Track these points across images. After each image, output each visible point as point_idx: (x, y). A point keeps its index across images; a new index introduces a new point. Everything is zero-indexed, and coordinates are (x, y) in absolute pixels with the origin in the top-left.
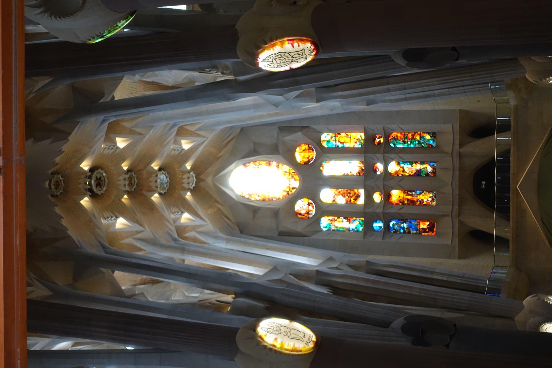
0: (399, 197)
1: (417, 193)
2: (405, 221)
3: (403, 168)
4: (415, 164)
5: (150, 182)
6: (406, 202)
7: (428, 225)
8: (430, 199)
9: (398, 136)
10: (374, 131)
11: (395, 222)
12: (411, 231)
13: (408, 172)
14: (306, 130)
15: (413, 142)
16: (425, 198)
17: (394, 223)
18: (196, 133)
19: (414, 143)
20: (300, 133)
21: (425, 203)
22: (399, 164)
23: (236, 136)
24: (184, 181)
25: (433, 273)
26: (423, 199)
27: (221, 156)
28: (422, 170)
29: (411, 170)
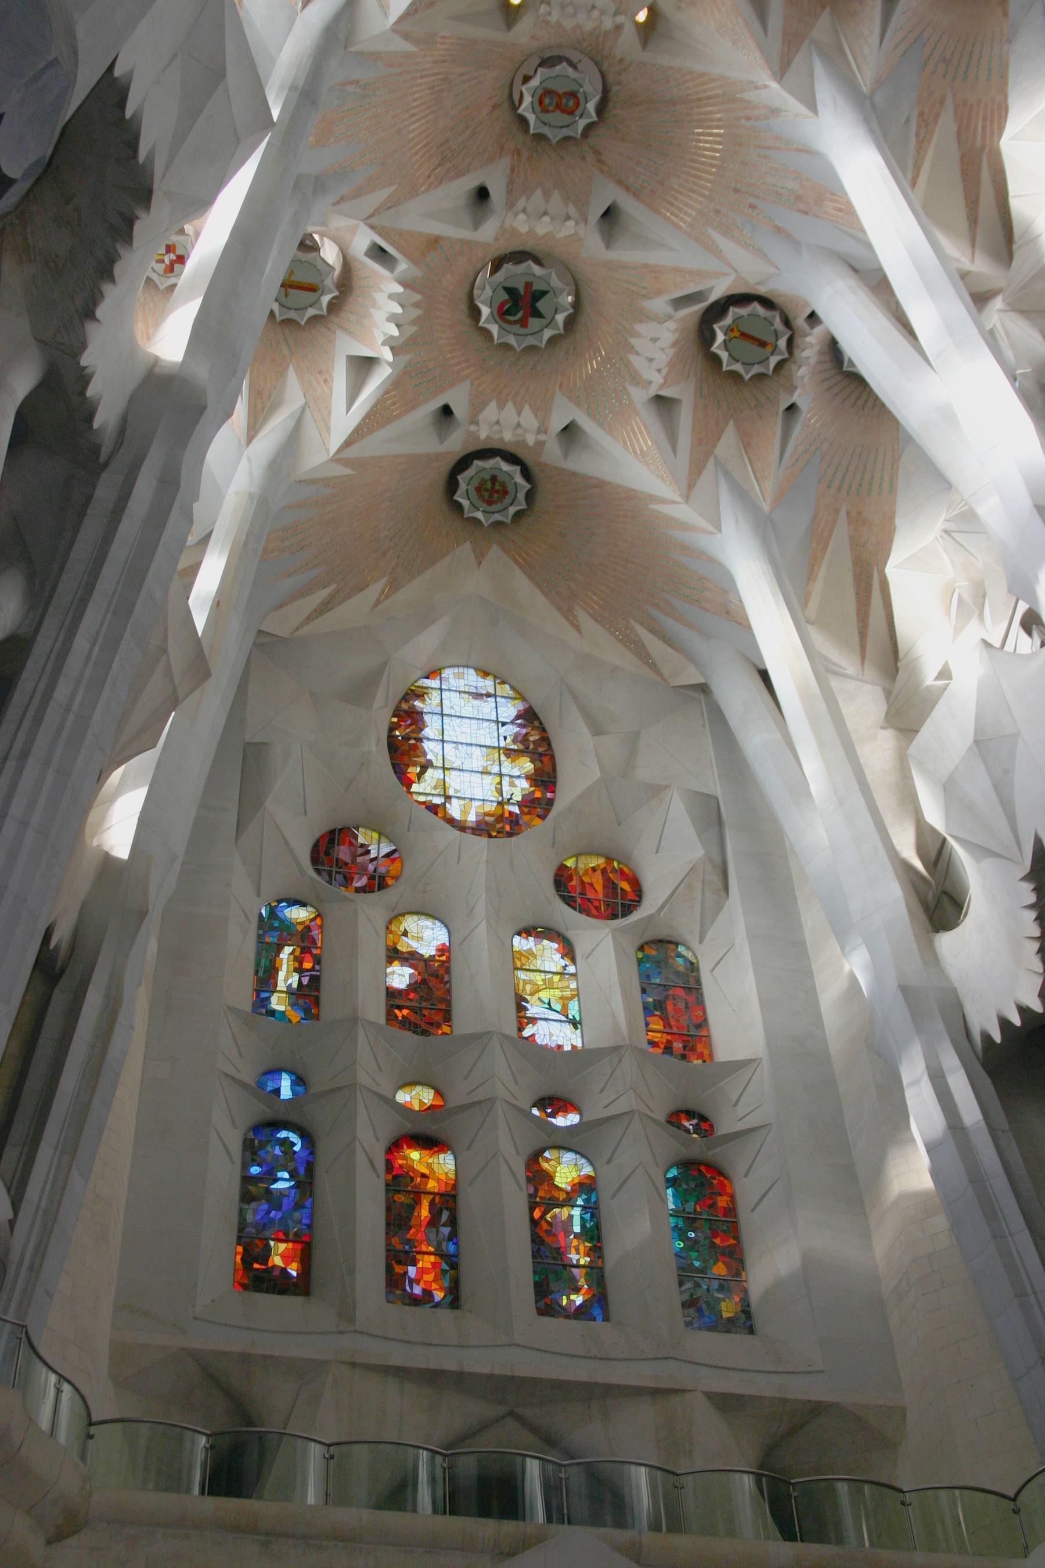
0: (424, 1176)
1: (444, 1244)
2: (305, 1182)
3: (569, 1201)
4: (591, 1249)
5: (547, 195)
6: (402, 1198)
7: (284, 1271)
8: (417, 1290)
9: (719, 1198)
10: (736, 1104)
11: (297, 1148)
12: (254, 1205)
13: (548, 1217)
14: (715, 879)
15: (698, 1251)
16: (422, 1271)
17: (294, 1144)
18: (706, 461)
19: (694, 1254)
20: (699, 852)
21: (398, 1269)
22: (585, 1186)
23: (661, 675)
24: (510, 407)
25: (70, 1149)
26: (420, 1265)
27: (577, 628)
28: (565, 1274)
29: (557, 1229)
